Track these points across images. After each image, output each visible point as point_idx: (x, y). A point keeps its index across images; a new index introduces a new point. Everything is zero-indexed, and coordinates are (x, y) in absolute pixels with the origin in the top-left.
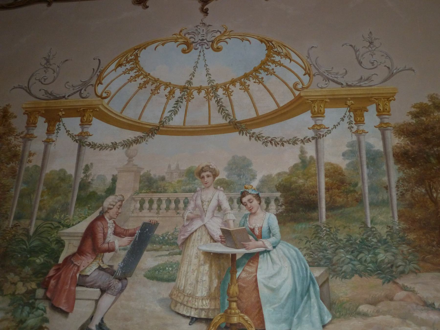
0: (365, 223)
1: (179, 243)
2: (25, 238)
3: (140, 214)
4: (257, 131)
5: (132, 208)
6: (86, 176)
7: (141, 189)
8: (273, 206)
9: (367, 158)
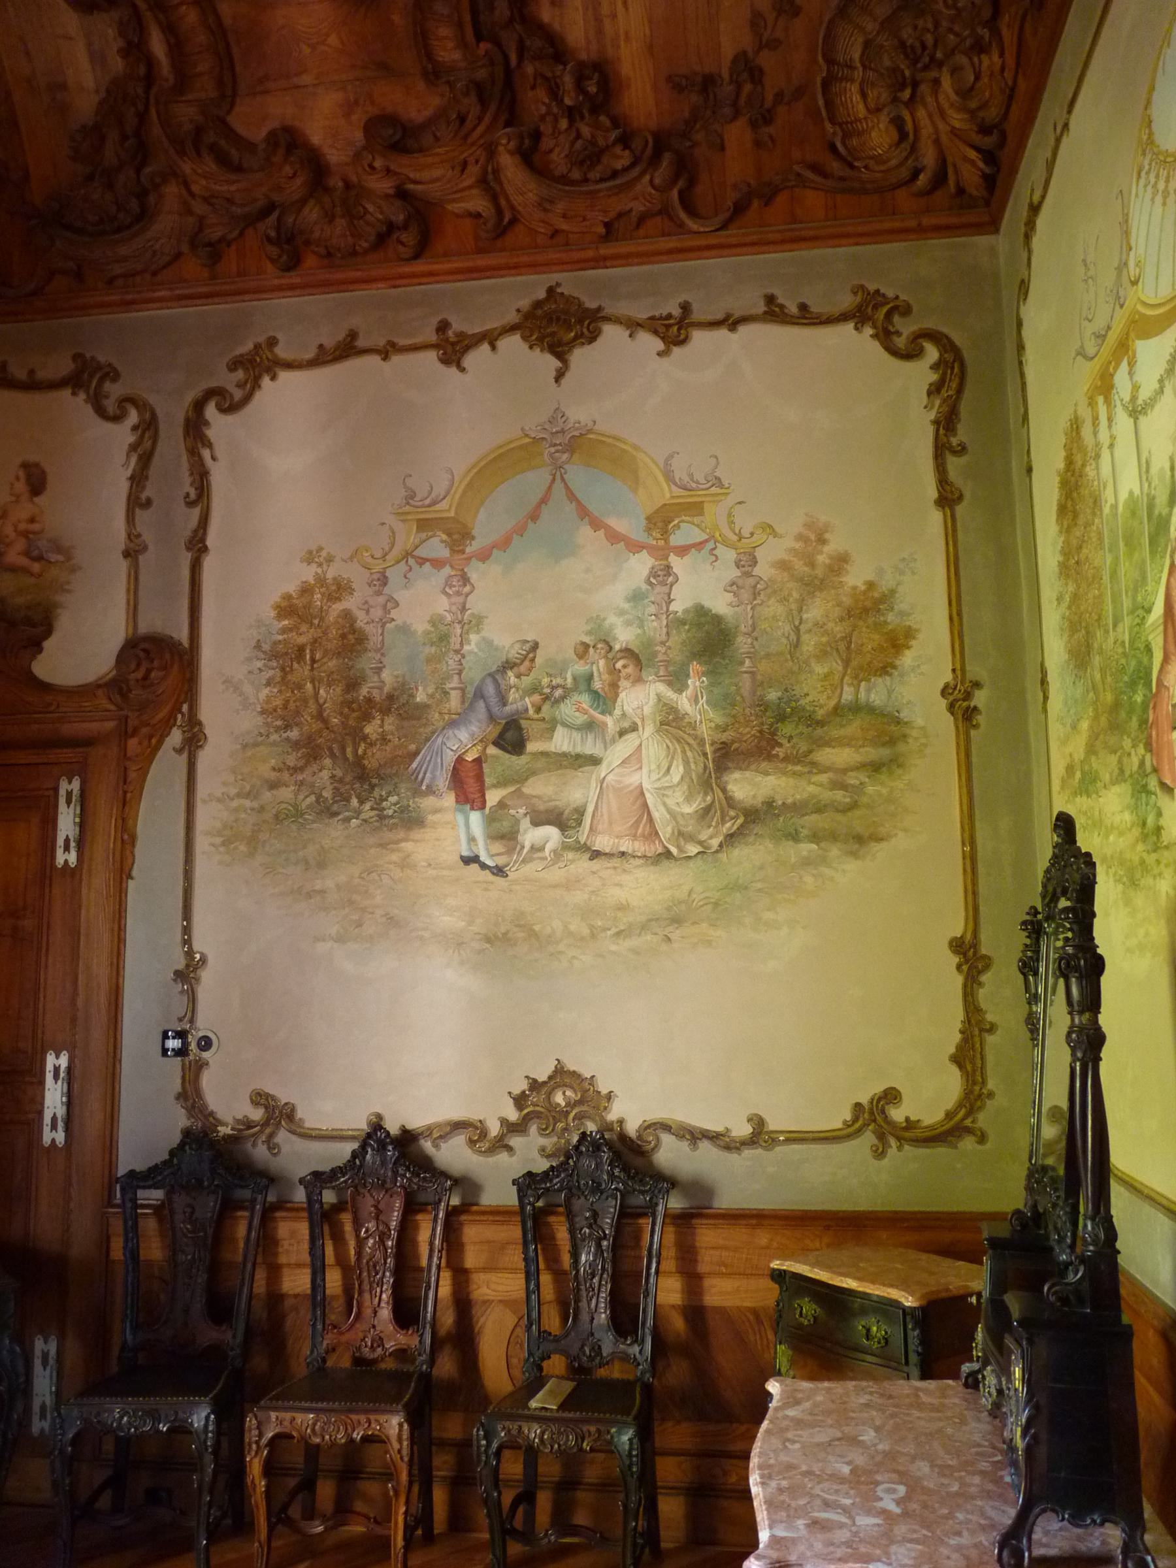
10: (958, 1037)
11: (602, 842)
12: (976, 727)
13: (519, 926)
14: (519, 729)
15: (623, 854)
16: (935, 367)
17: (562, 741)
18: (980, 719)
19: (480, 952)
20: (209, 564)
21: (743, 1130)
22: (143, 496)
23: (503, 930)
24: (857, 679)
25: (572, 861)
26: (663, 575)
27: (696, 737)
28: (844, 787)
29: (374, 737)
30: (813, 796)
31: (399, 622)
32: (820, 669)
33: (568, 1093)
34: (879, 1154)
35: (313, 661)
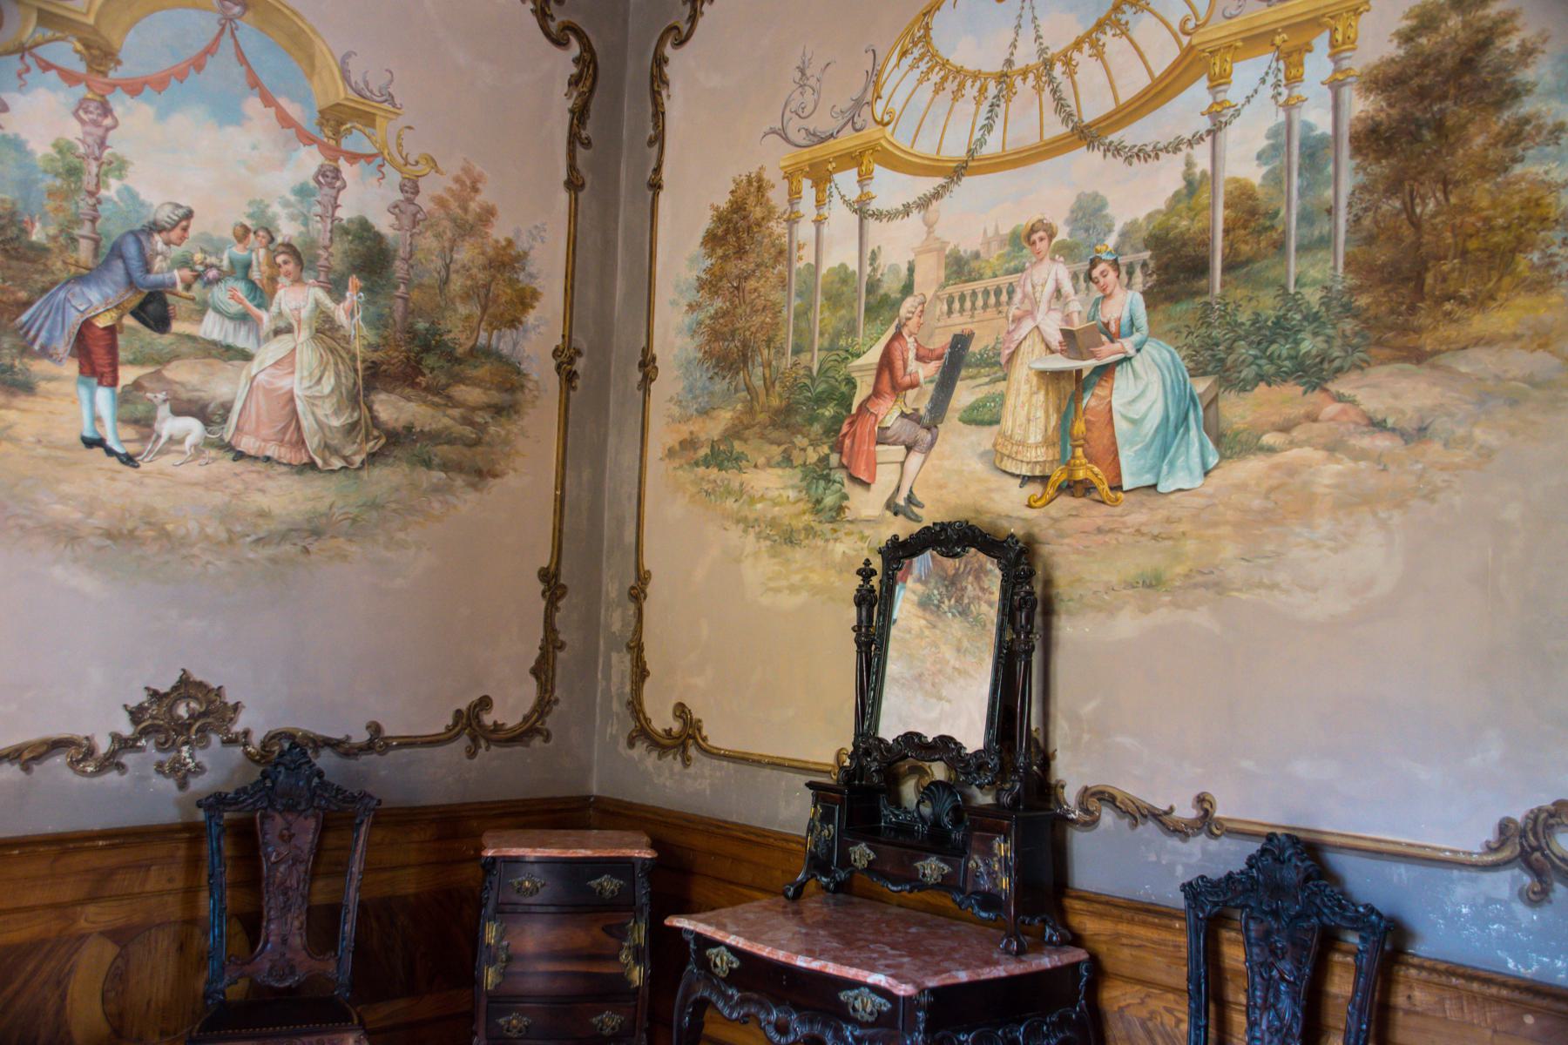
0: (1284, 287)
1: (1003, 360)
2: (808, 382)
3: (949, 322)
4: (1114, 137)
5: (938, 313)
6: (874, 270)
7: (948, 278)
8: (1138, 277)
9: (1301, 155)
10: (538, 652)
11: (247, 444)
12: (574, 388)
13: (149, 523)
14: (165, 304)
15: (268, 459)
16: (576, 61)
17: (212, 328)
18: (578, 383)
19: (100, 548)
23: (130, 525)
24: (492, 327)
25: (214, 460)
26: (330, 177)
27: (348, 352)
28: (472, 424)
30: (447, 428)
32: (463, 310)
33: (193, 705)
34: (472, 754)
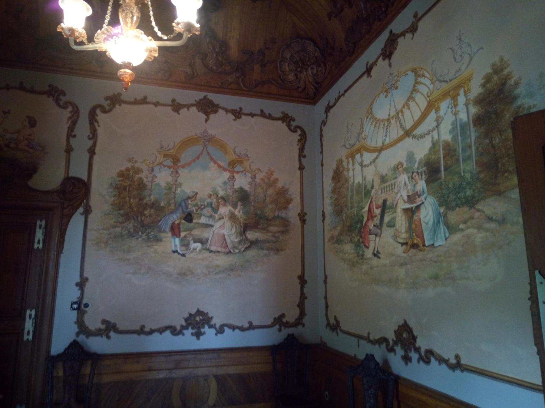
0: (460, 174)
1: (394, 206)
4: (414, 133)
9: (461, 129)
11: (213, 248)
15: (218, 252)
16: (300, 135)
17: (203, 220)
20: (96, 158)
21: (246, 325)
22: (73, 134)
26: (232, 178)
27: (239, 221)
28: (274, 236)
29: (147, 215)
31: (157, 182)
32: (270, 207)
33: (201, 317)
35: (129, 191)
